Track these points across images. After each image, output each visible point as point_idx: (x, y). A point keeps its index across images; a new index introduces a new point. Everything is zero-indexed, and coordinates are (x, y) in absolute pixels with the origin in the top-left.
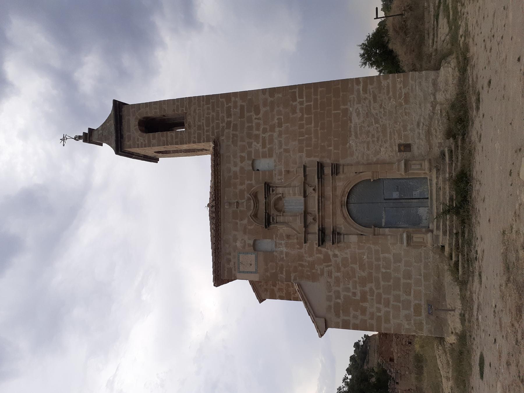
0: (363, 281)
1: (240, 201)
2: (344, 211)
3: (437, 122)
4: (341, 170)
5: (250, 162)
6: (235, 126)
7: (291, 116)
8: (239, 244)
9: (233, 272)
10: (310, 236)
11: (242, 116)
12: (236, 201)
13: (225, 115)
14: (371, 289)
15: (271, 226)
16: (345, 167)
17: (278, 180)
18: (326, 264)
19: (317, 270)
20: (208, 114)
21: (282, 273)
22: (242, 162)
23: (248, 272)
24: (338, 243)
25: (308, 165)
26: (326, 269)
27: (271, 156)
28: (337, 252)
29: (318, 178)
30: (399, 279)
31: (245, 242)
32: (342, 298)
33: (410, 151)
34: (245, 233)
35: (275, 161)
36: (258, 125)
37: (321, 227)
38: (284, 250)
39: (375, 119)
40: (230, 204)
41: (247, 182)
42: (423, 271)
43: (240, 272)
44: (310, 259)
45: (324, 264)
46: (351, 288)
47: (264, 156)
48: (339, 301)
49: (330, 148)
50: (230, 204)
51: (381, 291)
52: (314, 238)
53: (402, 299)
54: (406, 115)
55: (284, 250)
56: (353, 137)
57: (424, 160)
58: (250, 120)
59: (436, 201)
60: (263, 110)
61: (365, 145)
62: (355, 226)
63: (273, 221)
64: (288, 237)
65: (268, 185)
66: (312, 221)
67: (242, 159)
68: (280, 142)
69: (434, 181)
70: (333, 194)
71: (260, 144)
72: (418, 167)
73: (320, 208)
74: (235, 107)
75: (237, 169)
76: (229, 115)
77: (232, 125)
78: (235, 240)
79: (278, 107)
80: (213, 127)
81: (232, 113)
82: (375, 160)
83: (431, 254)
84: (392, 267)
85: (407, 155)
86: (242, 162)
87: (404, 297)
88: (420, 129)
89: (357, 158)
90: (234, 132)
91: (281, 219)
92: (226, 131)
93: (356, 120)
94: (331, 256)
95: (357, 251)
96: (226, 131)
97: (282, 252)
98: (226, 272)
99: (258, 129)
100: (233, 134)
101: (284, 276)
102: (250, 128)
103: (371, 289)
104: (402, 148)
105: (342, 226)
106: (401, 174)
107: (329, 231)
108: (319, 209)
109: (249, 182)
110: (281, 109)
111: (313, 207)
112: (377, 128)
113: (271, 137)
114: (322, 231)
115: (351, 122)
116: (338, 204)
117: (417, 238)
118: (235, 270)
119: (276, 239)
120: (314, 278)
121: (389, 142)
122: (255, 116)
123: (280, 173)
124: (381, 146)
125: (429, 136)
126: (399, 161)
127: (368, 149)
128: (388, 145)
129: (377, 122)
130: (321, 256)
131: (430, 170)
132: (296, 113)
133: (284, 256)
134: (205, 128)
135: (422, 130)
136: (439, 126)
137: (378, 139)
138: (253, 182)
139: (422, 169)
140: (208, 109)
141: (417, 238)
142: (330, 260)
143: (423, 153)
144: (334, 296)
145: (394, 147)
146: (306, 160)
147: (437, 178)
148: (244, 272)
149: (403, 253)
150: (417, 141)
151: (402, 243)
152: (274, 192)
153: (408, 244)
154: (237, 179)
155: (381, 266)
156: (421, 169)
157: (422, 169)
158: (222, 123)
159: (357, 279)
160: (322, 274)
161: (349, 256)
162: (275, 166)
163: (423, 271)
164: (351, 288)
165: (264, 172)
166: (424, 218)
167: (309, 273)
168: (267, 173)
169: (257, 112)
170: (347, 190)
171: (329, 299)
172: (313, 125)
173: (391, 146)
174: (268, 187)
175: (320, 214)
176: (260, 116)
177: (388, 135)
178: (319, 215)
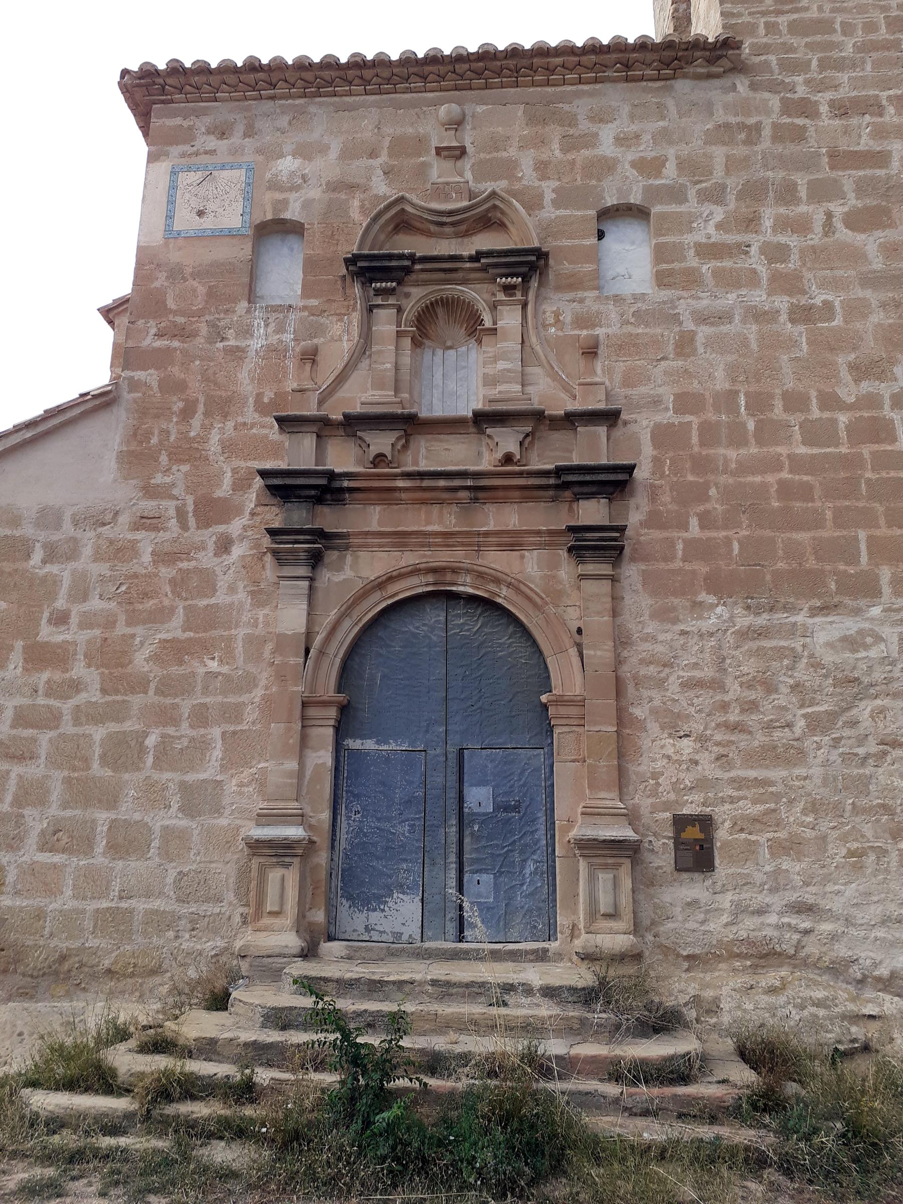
0: (111, 656)
1: (467, 164)
2: (414, 581)
3: (819, 994)
4: (591, 568)
5: (635, 198)
6: (799, 135)
7: (842, 360)
8: (287, 165)
9: (175, 150)
10: (308, 442)
11: (838, 159)
12: (470, 149)
13: (845, 92)
14: (76, 686)
15: (357, 289)
16: (605, 587)
17: (557, 315)
18: (190, 508)
19: (167, 471)
20: (848, 28)
21: (160, 335)
22: (641, 165)
23: (171, 202)
24: (275, 553)
25: (618, 432)
26: (170, 507)
27: (662, 279)
28: (238, 551)
29: (559, 471)
30: (112, 803)
31: (295, 188)
32: (49, 568)
33: (679, 869)
34: (334, 187)
35: (637, 298)
36: (801, 226)
37: (346, 484)
38: (256, 344)
39: (833, 716)
40: (457, 124)
41: (548, 189)
42: (140, 905)
43: (174, 173)
44: (214, 444)
45: (190, 500)
46: (85, 607)
47: (661, 254)
48: (38, 555)
49: (694, 522)
50: (457, 124)
51: (67, 728)
52: (300, 454)
53: (27, 812)
54: (851, 854)
55: (256, 344)
56: (744, 620)
57: (637, 929)
58: (822, 192)
59: (434, 983)
60: (870, 243)
61: (707, 673)
62: (347, 624)
63: (378, 292)
64: (310, 357)
65: (533, 267)
66: (374, 450)
67: (650, 167)
68: (724, 317)
69: (534, 975)
70: (487, 534)
71: (717, 237)
72: (604, 903)
73: (426, 483)
74: (880, 133)
75: (607, 147)
76: (841, 110)
77: (800, 121)
78: (304, 152)
79: (883, 305)
80: (791, 49)
81: (855, 121)
82: (638, 712)
83: (211, 945)
84: (167, 775)
85: (662, 857)
86: (641, 165)
87: (36, 822)
88: (781, 914)
89: (646, 638)
90: (767, 132)
91: (385, 324)
92: (775, 102)
93: (826, 631)
94: (221, 528)
95: (241, 632)
96: (775, 102)
97: (247, 332)
98: (178, 121)
99: (782, 225)
100: (758, 127)
101: (149, 341)
102: (787, 194)
103: (76, 686)
104: (693, 833)
105: (348, 573)
106: (571, 822)
107: (328, 519)
108: (422, 475)
109: (549, 196)
110: (877, 317)
112: (789, 725)
113: (753, 279)
114: (326, 490)
115: (815, 612)
116: (443, 557)
117: (283, 882)
118: (183, 155)
119: (305, 308)
120: (137, 459)
121: (719, 774)
122: (838, 209)
123: (581, 321)
124: (702, 739)
125: (746, 956)
126: (632, 817)
127: (688, 685)
128: (707, 767)
129: (815, 724)
130: (224, 489)
131: (588, 957)
132: (857, 381)
133: (232, 343)
134: (783, 20)
135: (778, 927)
136: (803, 1008)
137: (736, 728)
138: (549, 212)
139: (590, 920)
140: (870, 27)
141: (283, 882)
142: (204, 522)
143: (670, 925)
144: (56, 537)
145: (697, 797)
146: (642, 426)
147: (549, 992)
148: (173, 187)
149: (223, 822)
150: (726, 900)
151: (264, 818)
152: (501, 296)
153: (256, 846)
154: (565, 150)
155: (171, 731)
156: (593, 914)
157: (590, 920)
158: (807, 82)
159: (121, 629)
160: (150, 491)
161: (221, 598)
162: (618, 299)
163: (140, 905)
164: (85, 607)
165: (594, 256)
166: (375, 917)
167: (154, 440)
168: (589, 267)
169: (858, 221)
170: (504, 591)
171: (49, 518)
172: (802, 450)
173: (702, 784)
174: (526, 268)
175: (400, 484)
176: (843, 234)
177: (752, 774)
178: (394, 476)
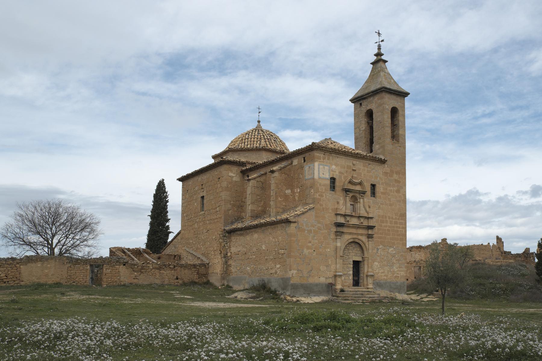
111: (354, 221)
116: (355, 236)
148: (319, 168)
